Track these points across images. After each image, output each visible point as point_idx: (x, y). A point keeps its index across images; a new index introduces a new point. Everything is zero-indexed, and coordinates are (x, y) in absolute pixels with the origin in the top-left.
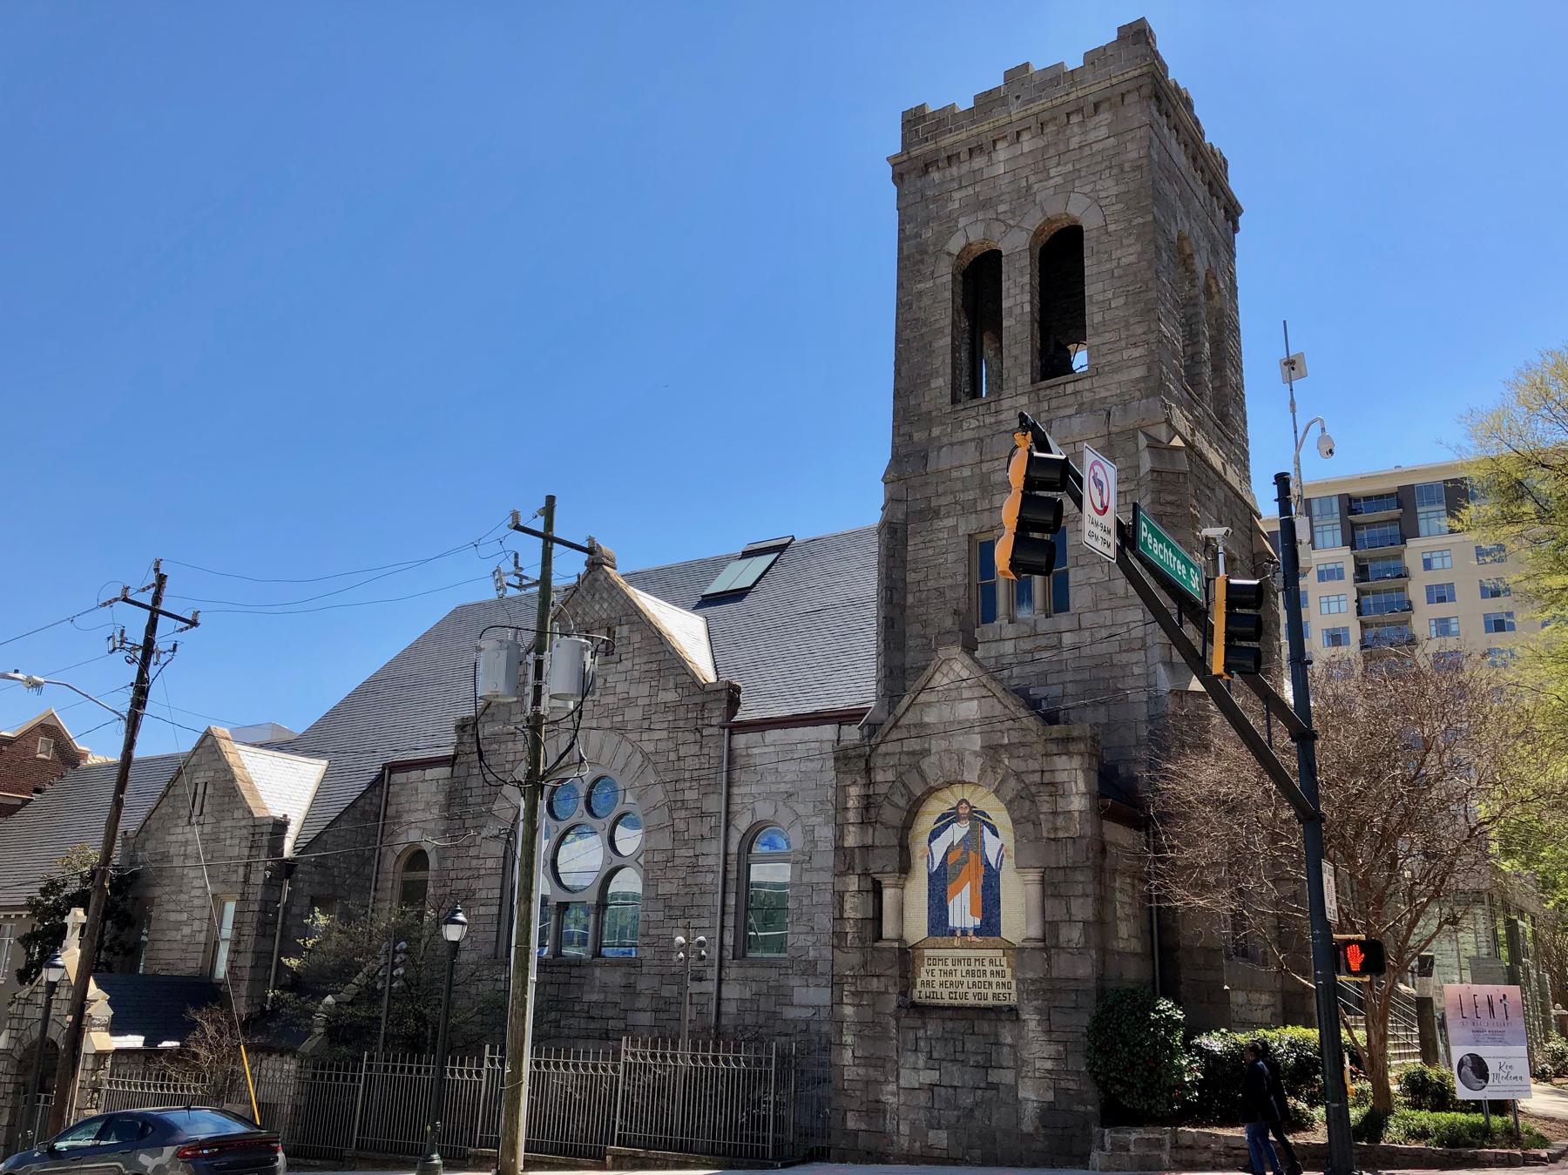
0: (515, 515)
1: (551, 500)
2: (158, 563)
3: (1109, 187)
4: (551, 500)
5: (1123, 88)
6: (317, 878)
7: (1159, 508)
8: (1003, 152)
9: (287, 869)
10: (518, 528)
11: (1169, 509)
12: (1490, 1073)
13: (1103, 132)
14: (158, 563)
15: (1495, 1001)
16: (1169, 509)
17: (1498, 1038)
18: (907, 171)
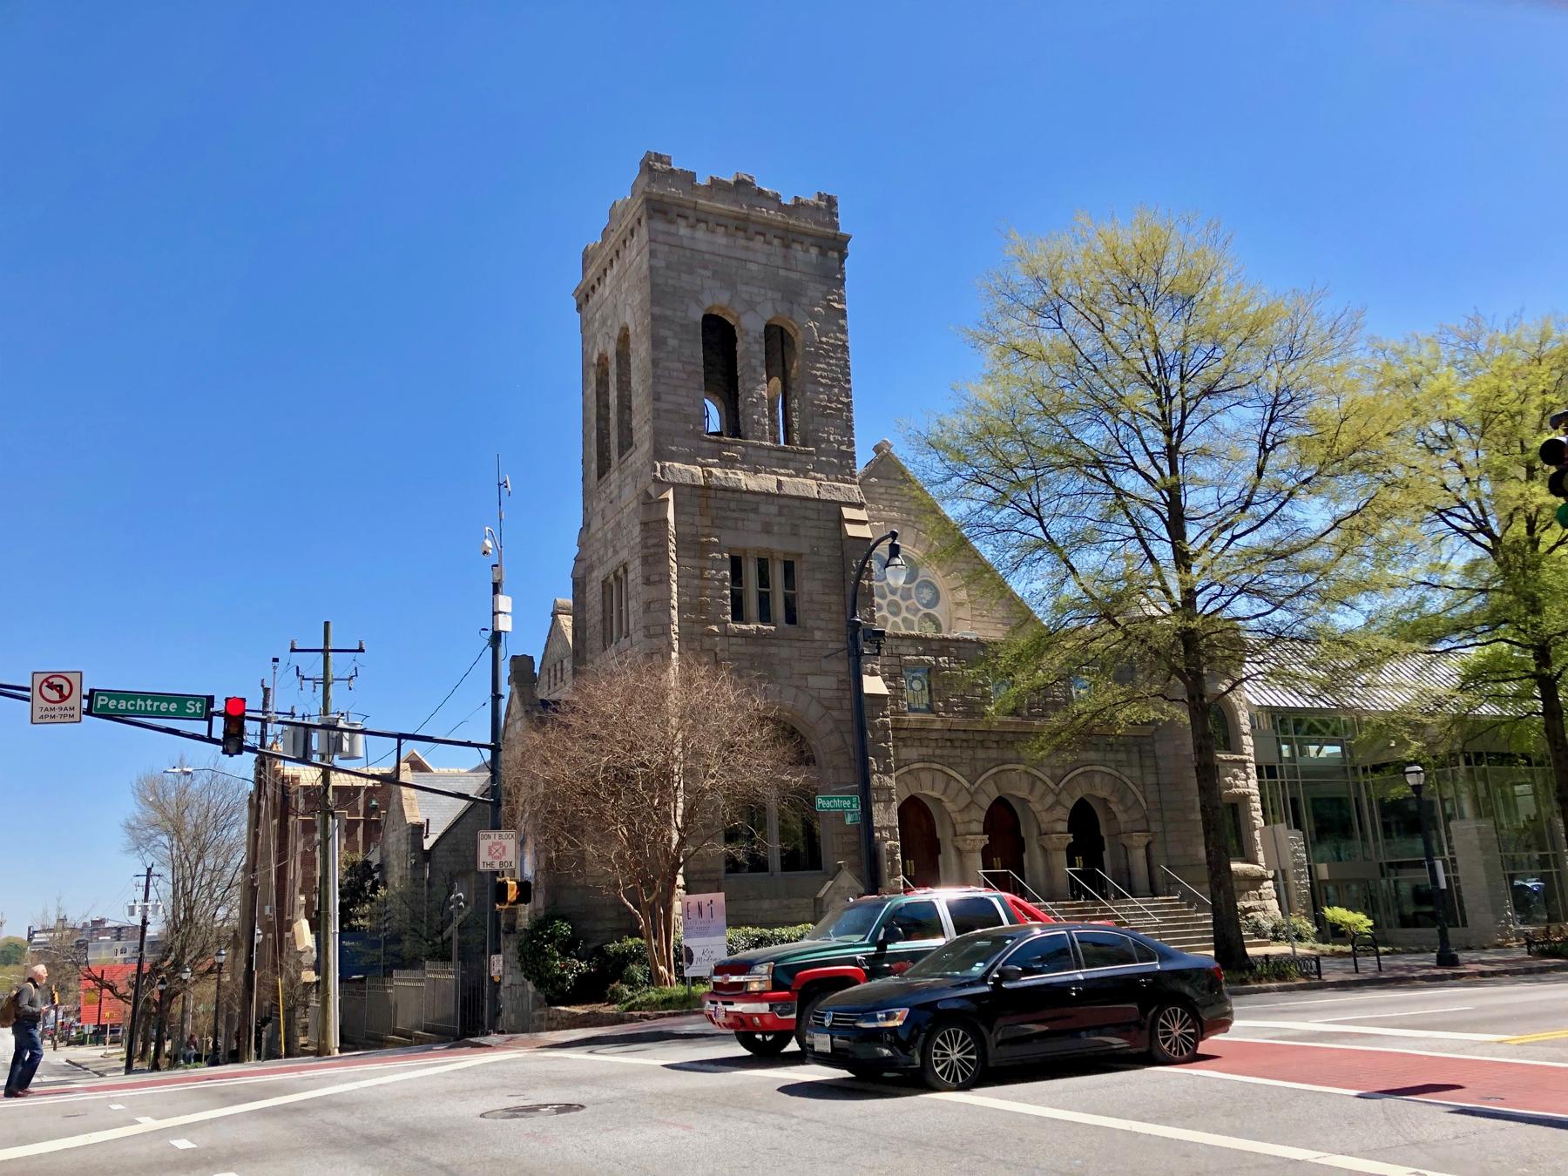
0: (293, 643)
1: (327, 624)
2: (263, 681)
3: (638, 297)
4: (327, 624)
5: (638, 215)
6: (452, 859)
7: (646, 551)
8: (608, 280)
9: (428, 855)
10: (293, 650)
11: (652, 551)
12: (695, 958)
13: (634, 253)
14: (263, 681)
15: (704, 906)
16: (652, 551)
17: (703, 932)
18: (584, 297)
